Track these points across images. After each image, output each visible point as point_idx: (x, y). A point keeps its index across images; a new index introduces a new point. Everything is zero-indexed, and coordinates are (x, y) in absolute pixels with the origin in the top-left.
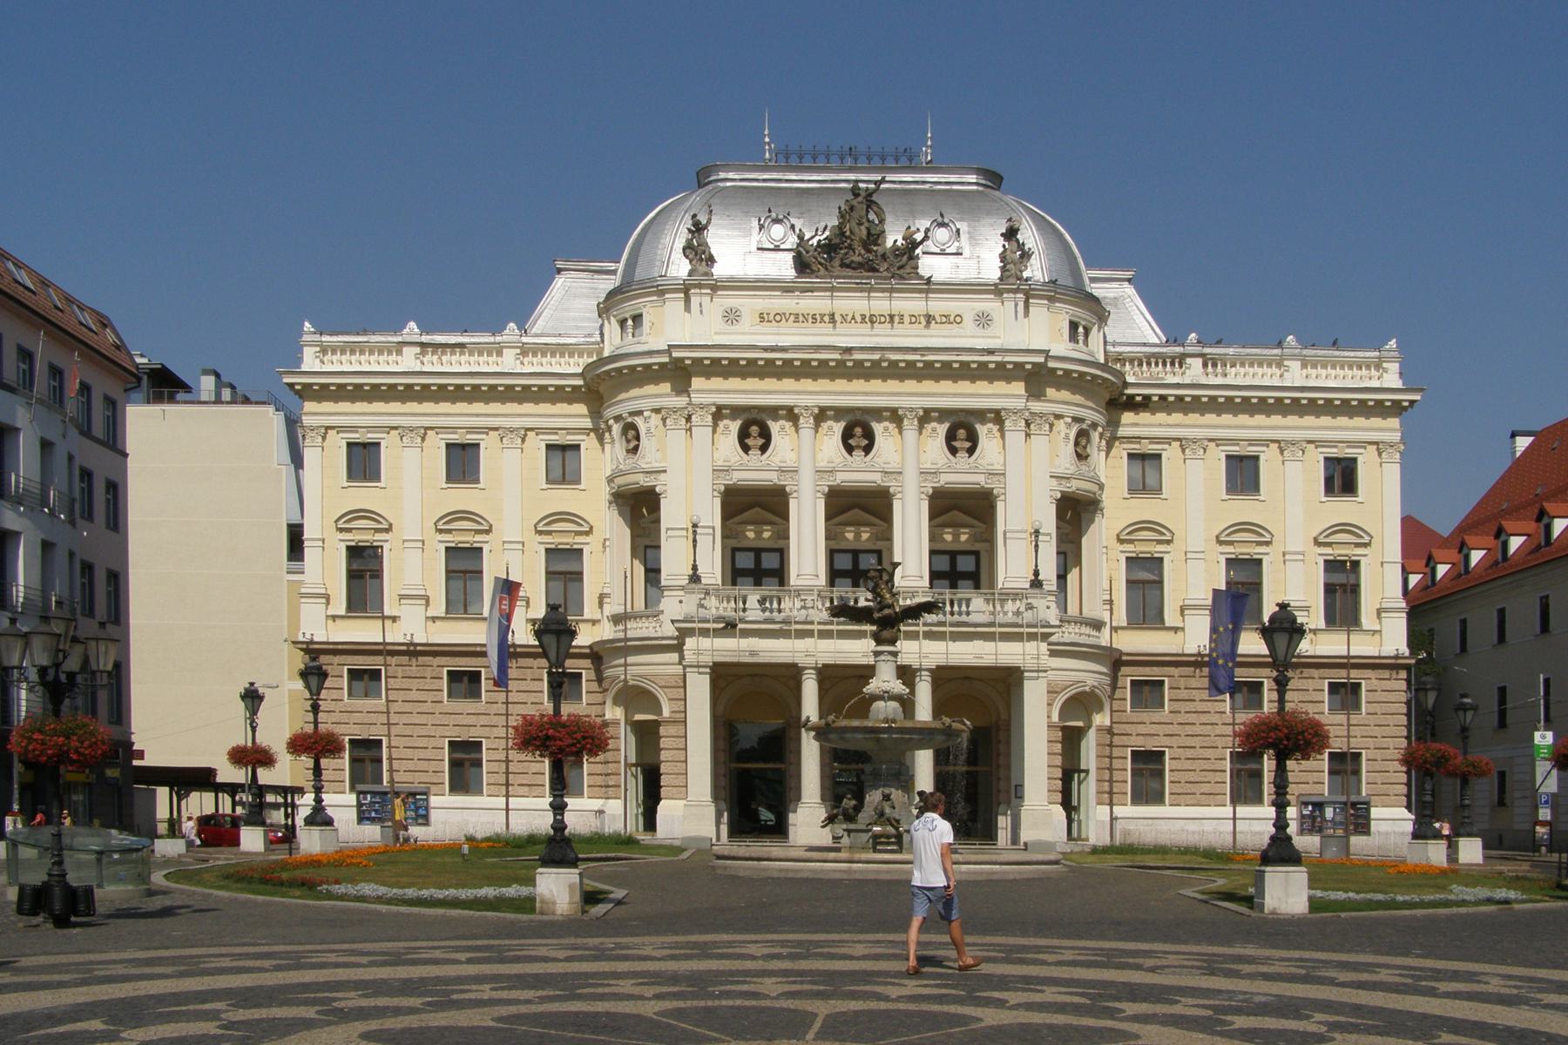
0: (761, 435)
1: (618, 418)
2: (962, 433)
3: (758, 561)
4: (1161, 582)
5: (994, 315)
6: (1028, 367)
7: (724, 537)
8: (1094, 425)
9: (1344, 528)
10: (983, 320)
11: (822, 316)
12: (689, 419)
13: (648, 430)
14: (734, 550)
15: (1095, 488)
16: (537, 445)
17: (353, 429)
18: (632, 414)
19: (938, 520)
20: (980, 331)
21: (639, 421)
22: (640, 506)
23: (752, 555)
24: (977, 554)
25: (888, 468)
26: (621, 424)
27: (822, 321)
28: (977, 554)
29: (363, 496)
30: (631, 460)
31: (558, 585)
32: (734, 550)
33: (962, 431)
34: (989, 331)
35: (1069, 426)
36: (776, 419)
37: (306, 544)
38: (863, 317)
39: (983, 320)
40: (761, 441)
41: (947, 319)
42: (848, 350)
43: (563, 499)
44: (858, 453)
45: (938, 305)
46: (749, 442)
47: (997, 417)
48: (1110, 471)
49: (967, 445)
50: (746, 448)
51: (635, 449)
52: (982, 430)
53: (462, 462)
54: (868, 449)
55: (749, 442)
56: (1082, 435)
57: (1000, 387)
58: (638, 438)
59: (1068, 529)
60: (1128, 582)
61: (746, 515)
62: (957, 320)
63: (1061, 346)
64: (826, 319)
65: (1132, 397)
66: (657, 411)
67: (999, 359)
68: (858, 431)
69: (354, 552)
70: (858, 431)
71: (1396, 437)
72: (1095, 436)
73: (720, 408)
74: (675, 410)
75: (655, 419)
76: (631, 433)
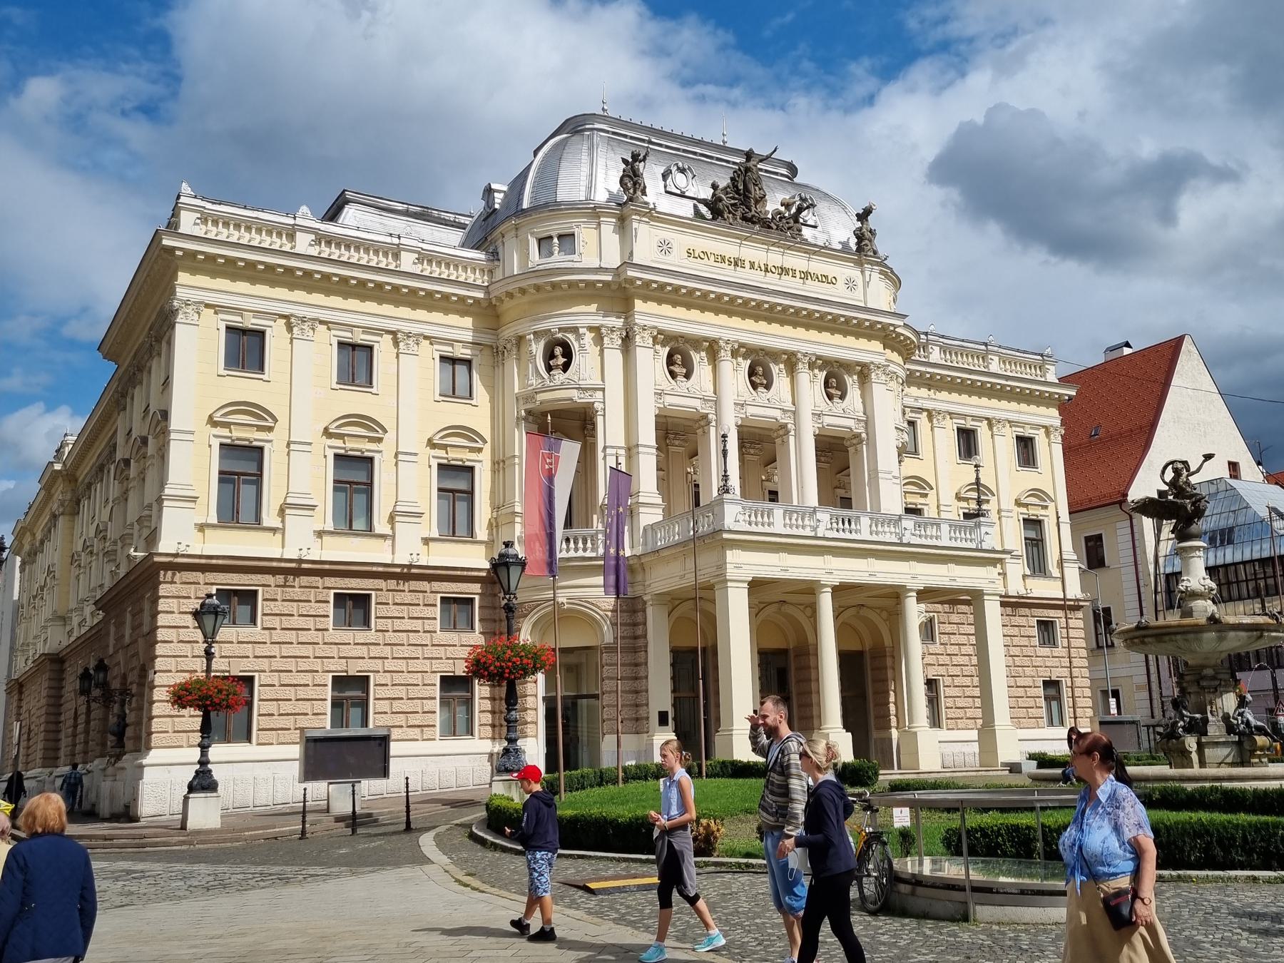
1: (537, 334)
10: (850, 284)
13: (582, 347)
16: (428, 355)
17: (238, 311)
20: (848, 293)
21: (571, 337)
29: (244, 387)
30: (559, 377)
33: (835, 377)
36: (697, 350)
37: (173, 436)
43: (458, 413)
45: (818, 266)
46: (676, 369)
47: (864, 372)
50: (673, 375)
51: (566, 367)
53: (356, 362)
57: (863, 343)
62: (832, 281)
66: (591, 329)
69: (228, 449)
71: (1057, 423)
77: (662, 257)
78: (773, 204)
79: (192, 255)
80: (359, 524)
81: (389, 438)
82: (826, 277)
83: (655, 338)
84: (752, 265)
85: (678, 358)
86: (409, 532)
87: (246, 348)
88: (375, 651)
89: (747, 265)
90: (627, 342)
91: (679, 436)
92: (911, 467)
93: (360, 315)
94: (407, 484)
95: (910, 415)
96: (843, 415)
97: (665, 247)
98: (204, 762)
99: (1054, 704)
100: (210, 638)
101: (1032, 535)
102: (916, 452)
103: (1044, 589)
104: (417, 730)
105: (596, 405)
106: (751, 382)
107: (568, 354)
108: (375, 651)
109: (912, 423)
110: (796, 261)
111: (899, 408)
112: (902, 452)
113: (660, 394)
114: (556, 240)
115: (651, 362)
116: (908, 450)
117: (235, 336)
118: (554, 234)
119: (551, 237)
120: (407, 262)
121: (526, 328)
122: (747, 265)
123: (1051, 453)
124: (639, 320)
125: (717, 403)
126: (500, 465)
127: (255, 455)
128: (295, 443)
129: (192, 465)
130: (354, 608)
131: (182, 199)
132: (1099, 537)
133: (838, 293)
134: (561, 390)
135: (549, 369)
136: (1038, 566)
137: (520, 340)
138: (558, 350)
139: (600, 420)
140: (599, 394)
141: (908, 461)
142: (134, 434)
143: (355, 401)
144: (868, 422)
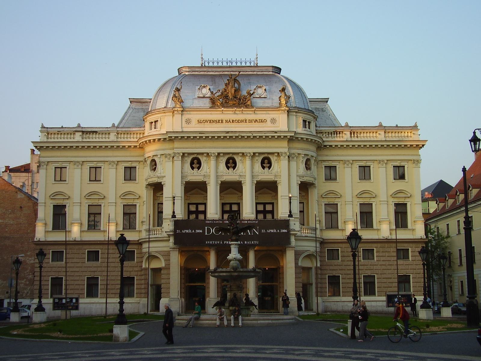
0: (198, 163)
2: (266, 161)
3: (197, 208)
4: (337, 213)
5: (277, 119)
6: (289, 137)
7: (185, 199)
8: (312, 156)
9: (400, 192)
11: (219, 121)
12: (173, 157)
14: (189, 204)
15: (313, 179)
18: (153, 156)
19: (258, 192)
20: (273, 125)
22: (157, 188)
23: (195, 206)
24: (273, 204)
25: (241, 174)
28: (273, 204)
30: (152, 173)
31: (127, 217)
32: (189, 204)
34: (275, 125)
35: (303, 157)
38: (233, 121)
39: (273, 121)
40: (198, 165)
41: (262, 121)
42: (228, 132)
43: (129, 186)
44: (231, 169)
46: (194, 166)
48: (318, 174)
49: (268, 165)
51: (155, 169)
52: (273, 159)
54: (234, 168)
55: (194, 166)
56: (308, 160)
58: (156, 165)
59: (304, 194)
60: (325, 213)
61: (192, 192)
63: (300, 129)
64: (220, 121)
65: (325, 146)
67: (279, 135)
68: (231, 161)
70: (231, 161)
72: (312, 161)
73: (184, 154)
76: (153, 163)
78: (244, 93)
85: (195, 161)
88: (99, 269)
98: (40, 302)
104: (114, 295)
108: (99, 269)
110: (248, 115)
114: (154, 123)
119: (153, 122)
120: (113, 137)
121: (147, 155)
122: (224, 121)
130: (94, 256)
140: (164, 179)
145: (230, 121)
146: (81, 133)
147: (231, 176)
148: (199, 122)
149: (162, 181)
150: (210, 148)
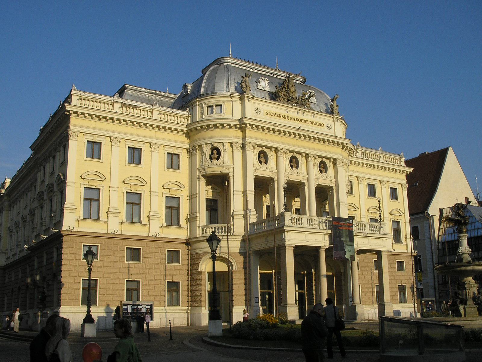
10: (329, 127)
26: (210, 146)
27: (285, 118)
29: (93, 165)
30: (215, 161)
41: (321, 125)
43: (173, 175)
47: (335, 161)
49: (325, 170)
50: (261, 162)
51: (218, 159)
53: (135, 155)
62: (321, 125)
64: (286, 117)
74: (237, 143)
75: (228, 146)
77: (256, 115)
79: (76, 113)
80: (136, 220)
81: (149, 184)
82: (320, 124)
83: (254, 147)
84: (291, 118)
86: (155, 224)
87: (94, 149)
89: (289, 118)
90: (243, 147)
91: (263, 186)
92: (352, 199)
93: (138, 136)
94: (154, 206)
95: (351, 179)
96: (326, 180)
97: (258, 111)
99: (402, 294)
100: (90, 264)
101: (396, 227)
102: (352, 193)
103: (400, 249)
104: (158, 303)
105: (230, 174)
106: (290, 165)
107: (219, 153)
109: (351, 182)
110: (308, 116)
111: (347, 176)
112: (348, 193)
113: (256, 170)
115: (252, 156)
116: (350, 192)
117: (90, 145)
118: (214, 105)
122: (289, 118)
123: (403, 195)
124: (248, 140)
125: (278, 174)
126: (192, 197)
127: (96, 191)
128: (112, 187)
129: (74, 196)
131: (73, 91)
132: (417, 227)
133: (325, 130)
134: (216, 168)
135: (211, 159)
136: (397, 239)
137: (200, 146)
138: (215, 152)
139: (232, 180)
141: (350, 197)
142: (47, 182)
143: (134, 170)
144: (337, 183)
145: (294, 119)
146: (120, 105)
147: (297, 176)
148: (268, 113)
149: (230, 172)
150: (280, 143)
